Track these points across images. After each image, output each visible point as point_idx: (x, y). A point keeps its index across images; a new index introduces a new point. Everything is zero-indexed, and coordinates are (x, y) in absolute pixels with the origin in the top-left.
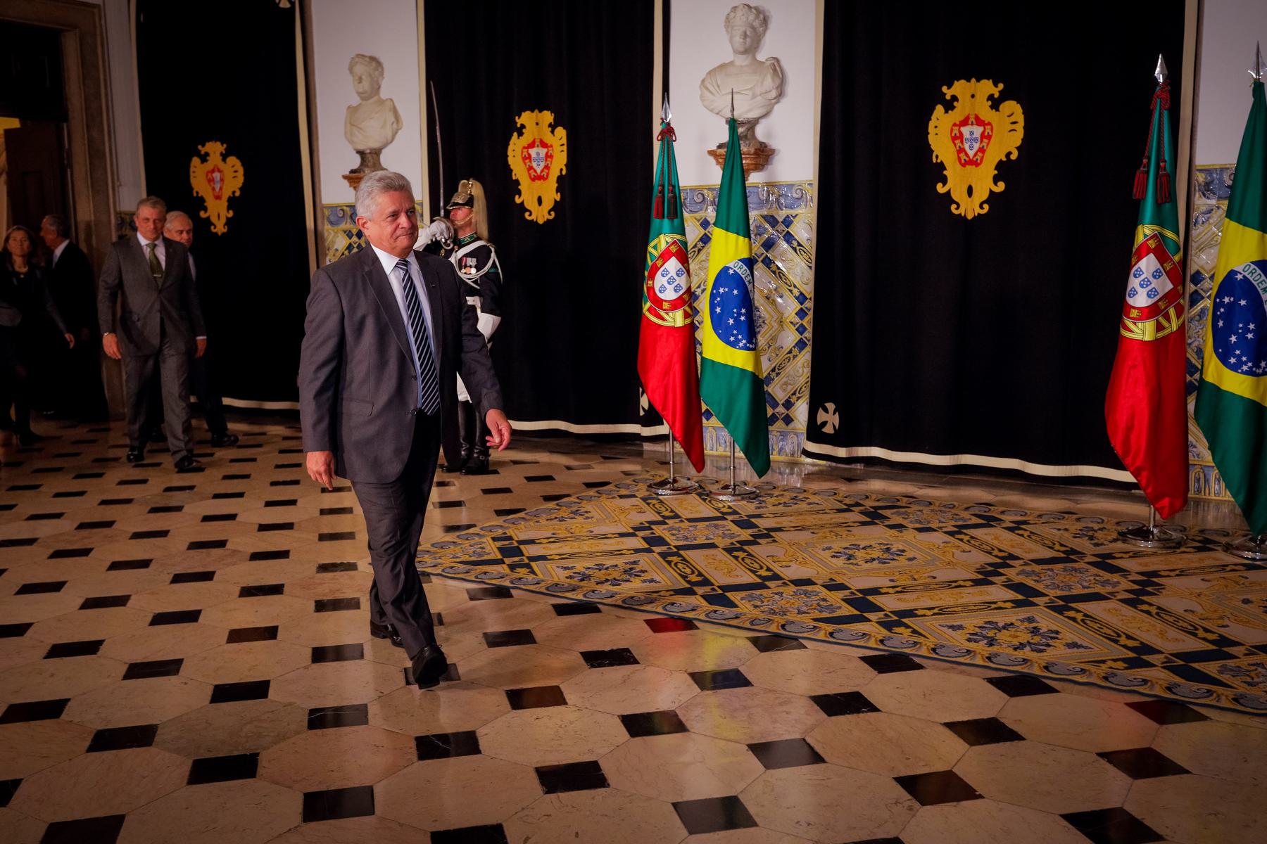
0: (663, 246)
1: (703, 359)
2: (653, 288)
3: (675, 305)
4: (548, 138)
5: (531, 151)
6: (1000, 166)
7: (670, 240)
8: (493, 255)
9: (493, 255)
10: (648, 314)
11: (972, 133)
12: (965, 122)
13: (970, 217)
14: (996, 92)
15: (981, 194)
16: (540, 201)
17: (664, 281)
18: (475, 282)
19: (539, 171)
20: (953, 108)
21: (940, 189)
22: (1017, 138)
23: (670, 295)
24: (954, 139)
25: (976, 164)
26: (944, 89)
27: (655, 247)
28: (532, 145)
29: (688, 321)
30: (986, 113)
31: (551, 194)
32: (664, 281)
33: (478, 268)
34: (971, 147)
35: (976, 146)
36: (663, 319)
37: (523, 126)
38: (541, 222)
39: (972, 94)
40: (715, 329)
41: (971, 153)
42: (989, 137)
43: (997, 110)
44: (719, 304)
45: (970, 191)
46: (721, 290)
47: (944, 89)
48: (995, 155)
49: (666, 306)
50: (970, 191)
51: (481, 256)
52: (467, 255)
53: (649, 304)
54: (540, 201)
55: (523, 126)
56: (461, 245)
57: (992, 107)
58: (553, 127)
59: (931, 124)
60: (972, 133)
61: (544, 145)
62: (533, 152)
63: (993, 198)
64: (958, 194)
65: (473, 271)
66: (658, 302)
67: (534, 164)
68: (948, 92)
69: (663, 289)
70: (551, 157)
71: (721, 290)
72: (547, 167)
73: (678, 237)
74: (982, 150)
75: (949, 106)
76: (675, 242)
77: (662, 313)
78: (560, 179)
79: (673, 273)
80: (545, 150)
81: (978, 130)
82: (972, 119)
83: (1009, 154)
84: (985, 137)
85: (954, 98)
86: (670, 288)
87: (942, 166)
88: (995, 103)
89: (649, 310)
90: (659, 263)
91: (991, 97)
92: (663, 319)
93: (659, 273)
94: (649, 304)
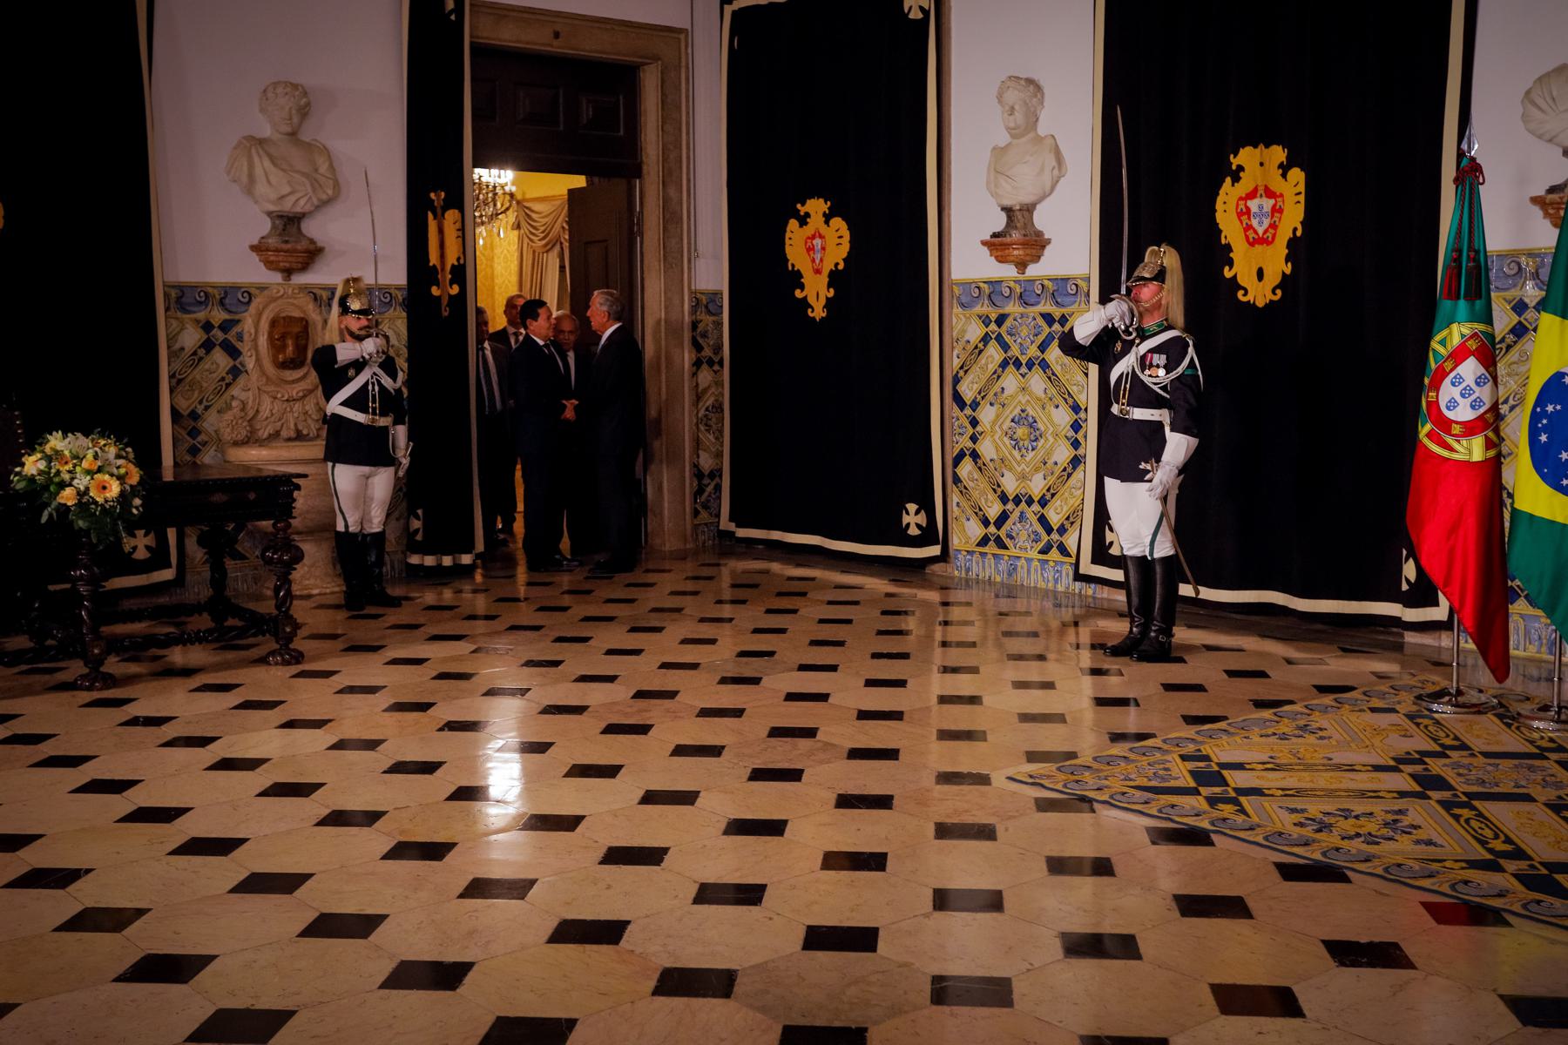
0: (1456, 340)
1: (1515, 512)
2: (1437, 401)
3: (1470, 429)
4: (1277, 184)
5: (1249, 203)
7: (1466, 331)
8: (1191, 350)
9: (1191, 350)
10: (1426, 441)
16: (1260, 274)
17: (1455, 392)
18: (1164, 388)
19: (1260, 232)
23: (1463, 413)
27: (1443, 343)
28: (1252, 195)
29: (1491, 453)
31: (1276, 263)
32: (1455, 392)
33: (1169, 368)
36: (1451, 449)
37: (1241, 168)
38: (1260, 304)
40: (1537, 466)
44: (1545, 429)
46: (1550, 408)
49: (1456, 429)
51: (1172, 352)
52: (1152, 351)
53: (1428, 427)
54: (1260, 274)
55: (1241, 168)
56: (1143, 335)
58: (1285, 169)
61: (1269, 193)
62: (1253, 205)
65: (1162, 372)
66: (1445, 424)
67: (1255, 223)
69: (1453, 404)
70: (1281, 211)
71: (1550, 408)
72: (1273, 226)
73: (1480, 327)
76: (1474, 336)
77: (1450, 440)
78: (1293, 243)
79: (1470, 380)
80: (1272, 202)
86: (1464, 404)
89: (1429, 435)
90: (1448, 365)
92: (1451, 449)
93: (1447, 381)
94: (1428, 427)
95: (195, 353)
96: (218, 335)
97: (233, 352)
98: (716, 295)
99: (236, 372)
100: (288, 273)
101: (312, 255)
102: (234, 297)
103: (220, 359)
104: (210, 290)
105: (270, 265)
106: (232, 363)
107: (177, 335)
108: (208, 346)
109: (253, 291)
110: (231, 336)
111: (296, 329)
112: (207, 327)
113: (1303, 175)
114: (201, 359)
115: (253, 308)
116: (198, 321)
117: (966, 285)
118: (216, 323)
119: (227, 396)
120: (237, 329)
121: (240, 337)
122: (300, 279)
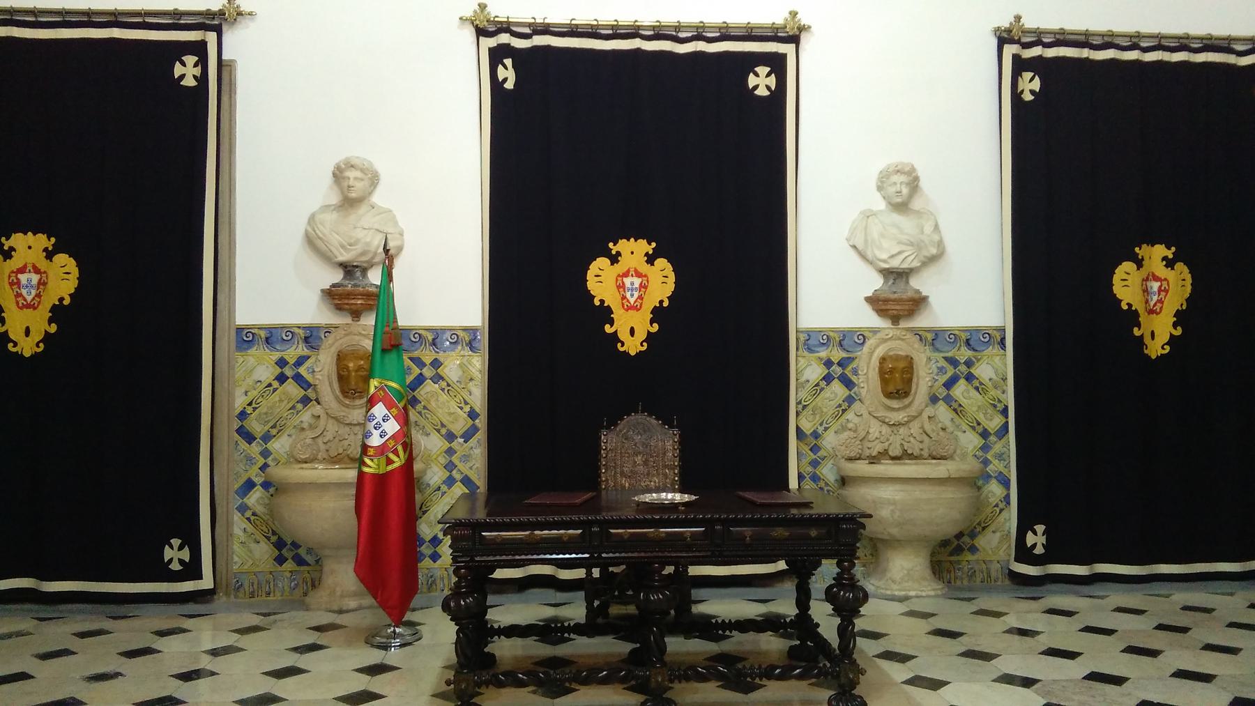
6: (655, 311)
11: (632, 284)
12: (626, 275)
13: (633, 353)
14: (650, 249)
15: (641, 335)
20: (617, 262)
21: (608, 329)
22: (670, 287)
24: (618, 287)
25: (636, 308)
26: (611, 245)
30: (645, 268)
34: (632, 295)
35: (636, 294)
39: (633, 250)
41: (632, 300)
42: (646, 287)
43: (652, 264)
45: (632, 332)
47: (611, 245)
48: (651, 302)
50: (632, 332)
57: (647, 262)
59: (590, 275)
60: (632, 284)
63: (650, 337)
64: (624, 335)
68: (614, 249)
74: (640, 297)
75: (614, 259)
81: (637, 281)
82: (632, 272)
83: (661, 302)
85: (619, 254)
87: (609, 310)
88: (651, 259)
91: (647, 254)
95: (817, 385)
96: (837, 370)
97: (848, 383)
99: (850, 400)
100: (895, 319)
101: (918, 303)
102: (850, 340)
103: (837, 389)
104: (832, 334)
105: (881, 312)
106: (847, 392)
107: (804, 370)
108: (828, 379)
109: (866, 334)
110: (848, 371)
111: (902, 365)
112: (828, 364)
113: (1186, 270)
114: (822, 389)
115: (866, 348)
116: (821, 359)
117: (810, 333)
118: (835, 359)
119: (842, 420)
120: (854, 365)
121: (855, 372)
122: (904, 324)
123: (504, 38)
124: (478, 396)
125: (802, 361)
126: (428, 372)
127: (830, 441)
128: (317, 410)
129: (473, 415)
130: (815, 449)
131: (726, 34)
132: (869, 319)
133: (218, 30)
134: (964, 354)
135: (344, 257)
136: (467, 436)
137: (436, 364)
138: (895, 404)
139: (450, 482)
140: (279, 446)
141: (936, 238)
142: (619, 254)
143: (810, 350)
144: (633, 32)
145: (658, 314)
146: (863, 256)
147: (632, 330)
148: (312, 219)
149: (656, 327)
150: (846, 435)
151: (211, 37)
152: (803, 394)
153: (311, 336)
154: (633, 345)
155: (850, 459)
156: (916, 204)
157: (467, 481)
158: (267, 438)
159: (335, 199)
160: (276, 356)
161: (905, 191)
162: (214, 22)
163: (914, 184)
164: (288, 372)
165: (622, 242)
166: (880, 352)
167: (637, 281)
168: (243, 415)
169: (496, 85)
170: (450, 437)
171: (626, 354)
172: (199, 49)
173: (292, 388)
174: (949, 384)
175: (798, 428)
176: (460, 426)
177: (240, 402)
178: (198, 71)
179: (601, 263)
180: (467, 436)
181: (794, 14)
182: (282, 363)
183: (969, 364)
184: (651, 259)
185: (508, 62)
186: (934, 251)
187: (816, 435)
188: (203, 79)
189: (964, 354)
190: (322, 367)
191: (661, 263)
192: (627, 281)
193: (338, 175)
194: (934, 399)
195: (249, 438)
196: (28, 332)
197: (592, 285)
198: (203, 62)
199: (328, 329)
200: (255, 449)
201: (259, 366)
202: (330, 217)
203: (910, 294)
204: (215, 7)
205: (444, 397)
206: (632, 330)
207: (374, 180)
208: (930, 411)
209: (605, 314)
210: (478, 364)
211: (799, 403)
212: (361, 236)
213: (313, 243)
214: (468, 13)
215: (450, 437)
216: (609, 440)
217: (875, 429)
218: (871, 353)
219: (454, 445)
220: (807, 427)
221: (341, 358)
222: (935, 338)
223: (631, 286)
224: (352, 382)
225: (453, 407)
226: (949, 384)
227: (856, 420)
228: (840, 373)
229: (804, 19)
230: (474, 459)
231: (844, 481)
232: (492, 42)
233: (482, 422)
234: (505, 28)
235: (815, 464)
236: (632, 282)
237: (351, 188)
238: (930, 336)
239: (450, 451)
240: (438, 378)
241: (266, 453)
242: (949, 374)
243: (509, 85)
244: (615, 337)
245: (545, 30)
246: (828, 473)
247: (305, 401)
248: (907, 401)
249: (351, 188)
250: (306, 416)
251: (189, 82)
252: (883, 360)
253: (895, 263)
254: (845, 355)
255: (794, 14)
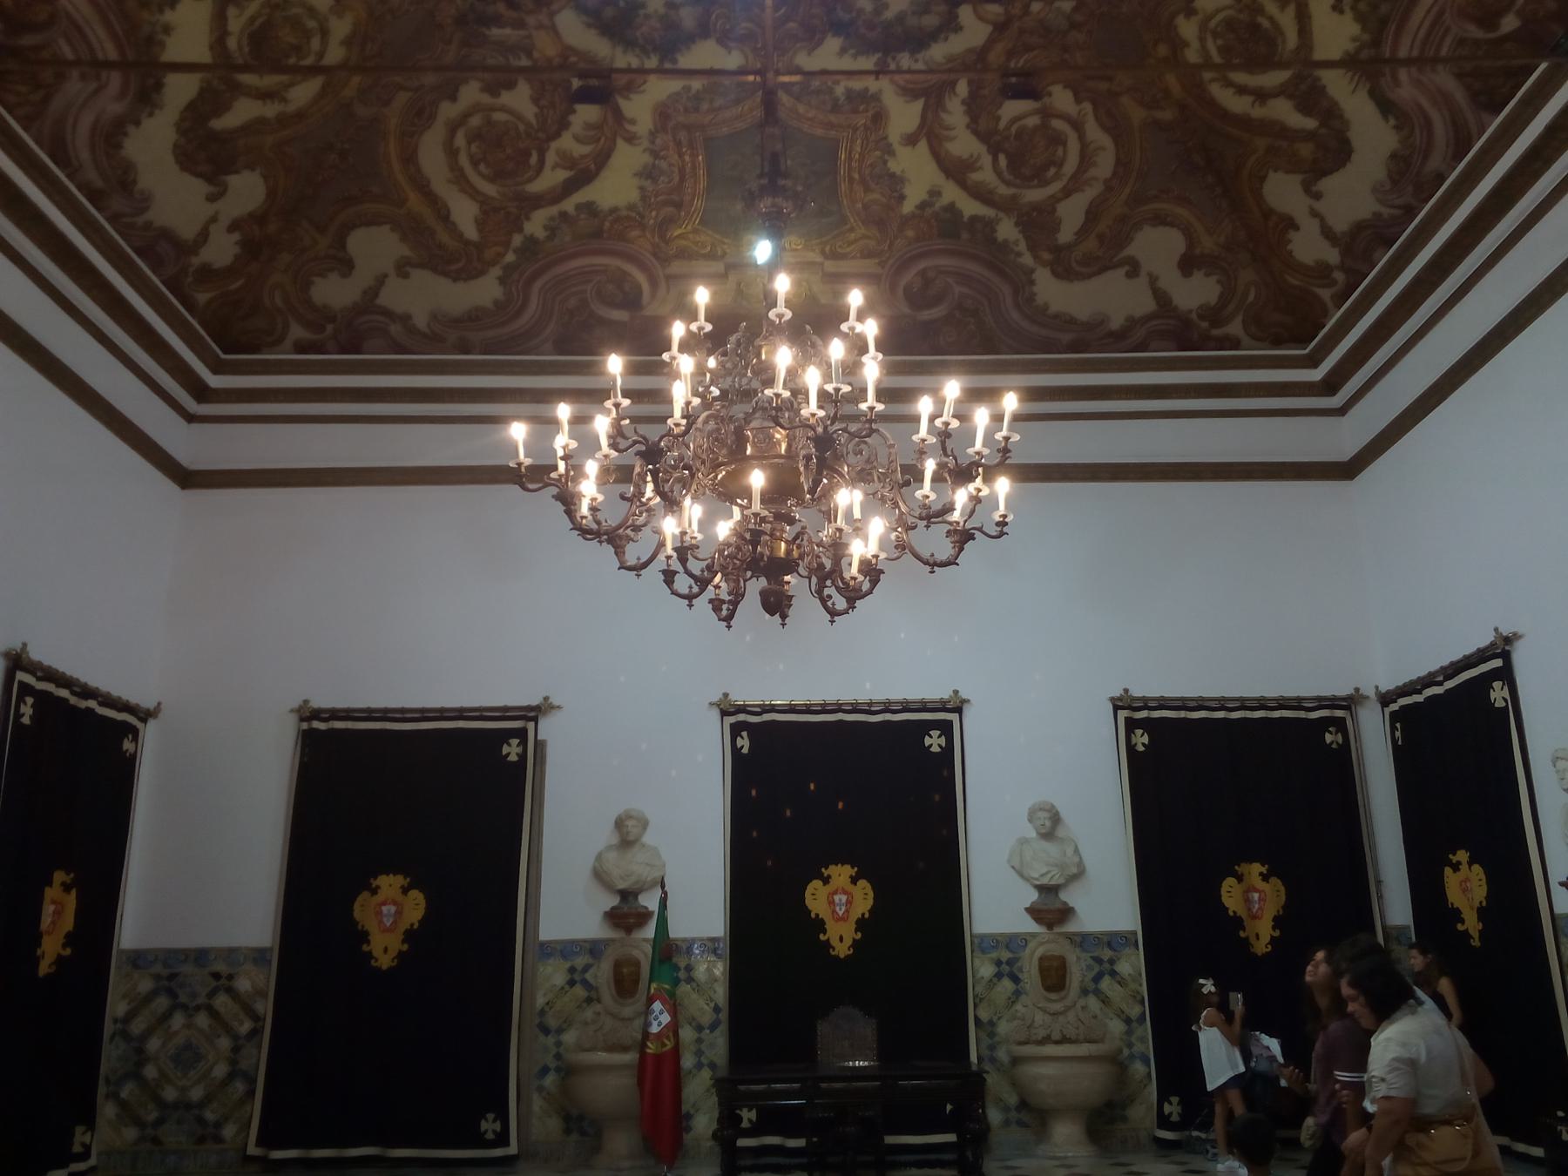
12: (835, 892)
14: (853, 871)
15: (848, 941)
21: (822, 937)
22: (870, 902)
25: (843, 919)
30: (850, 887)
39: (841, 873)
45: (841, 939)
50: (841, 939)
64: (835, 942)
68: (825, 872)
74: (847, 911)
75: (826, 880)
81: (844, 898)
84: (849, 902)
85: (829, 877)
87: (822, 922)
88: (854, 880)
96: (1006, 968)
97: (1016, 979)
98: (1134, 933)
99: (1017, 993)
100: (1050, 926)
101: (1066, 913)
102: (1013, 942)
103: (1007, 985)
105: (1038, 920)
107: (980, 969)
108: (999, 976)
112: (999, 963)
115: (1028, 951)
118: (1004, 960)
121: (1021, 970)
122: (1057, 930)
123: (742, 717)
124: (721, 993)
125: (977, 962)
126: (682, 975)
127: (1003, 1028)
128: (598, 1007)
129: (717, 1009)
130: (992, 1035)
131: (906, 707)
132: (1029, 926)
133: (535, 720)
134: (1107, 954)
135: (622, 885)
136: (713, 1027)
137: (689, 968)
138: (1053, 996)
139: (699, 1066)
140: (569, 1037)
141: (1076, 859)
142: (829, 877)
143: (983, 952)
144: (838, 708)
145: (861, 924)
146: (1021, 875)
147: (841, 938)
148: (599, 857)
149: (859, 935)
150: (1016, 1023)
151: (531, 725)
152: (979, 989)
153: (594, 949)
154: (842, 950)
155: (1021, 1043)
156: (1060, 832)
157: (712, 1066)
158: (560, 1031)
159: (615, 840)
160: (568, 965)
161: (1048, 823)
162: (533, 713)
163: (1056, 819)
164: (577, 977)
165: (832, 867)
166: (1040, 951)
167: (844, 898)
168: (542, 1012)
169: (736, 751)
170: (700, 1028)
171: (837, 958)
172: (522, 734)
173: (579, 991)
174: (1097, 978)
175: (976, 1017)
176: (707, 1018)
177: (540, 1001)
178: (519, 750)
179: (816, 884)
180: (713, 1027)
181: (956, 692)
182: (572, 970)
183: (1112, 962)
184: (854, 880)
185: (744, 734)
186: (1074, 870)
187: (992, 1023)
188: (523, 757)
189: (1107, 954)
190: (602, 974)
191: (863, 883)
192: (836, 898)
193: (619, 824)
194: (1085, 992)
195: (546, 1030)
196: (386, 950)
197: (809, 902)
198: (524, 742)
199: (607, 942)
200: (551, 1040)
201: (553, 974)
202: (612, 856)
203: (1058, 905)
204: (534, 702)
205: (694, 996)
206: (841, 938)
207: (645, 824)
208: (1082, 1002)
209: (820, 925)
210: (720, 969)
211: (975, 996)
212: (634, 867)
213: (600, 876)
214: (715, 699)
215: (700, 1028)
216: (823, 1028)
217: (1039, 1018)
218: (1033, 953)
219: (703, 1035)
220: (984, 1015)
221: (618, 965)
222: (1083, 941)
223: (839, 902)
224: (625, 982)
225: (702, 1003)
226: (1097, 978)
227: (1023, 1010)
228: (1008, 970)
229: (964, 695)
230: (718, 1046)
231: (1016, 1061)
232: (732, 719)
233: (724, 1016)
234: (742, 709)
235: (992, 1048)
236: (840, 898)
237: (627, 832)
238: (1078, 939)
239: (699, 1041)
240: (690, 980)
241: (559, 1044)
242: (1097, 969)
243: (745, 751)
244: (827, 944)
245: (773, 709)
246: (1002, 1055)
247: (589, 1000)
248: (1063, 994)
249: (627, 832)
250: (589, 1014)
251: (513, 758)
252: (1041, 959)
253: (1045, 881)
254: (1010, 955)
255: (956, 692)
